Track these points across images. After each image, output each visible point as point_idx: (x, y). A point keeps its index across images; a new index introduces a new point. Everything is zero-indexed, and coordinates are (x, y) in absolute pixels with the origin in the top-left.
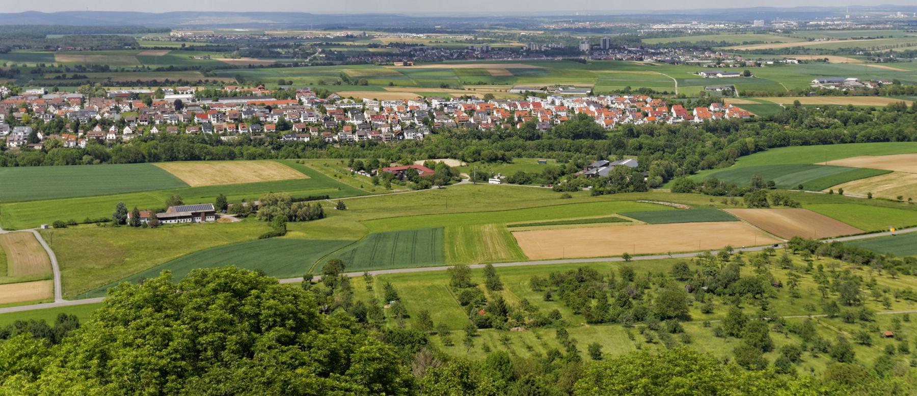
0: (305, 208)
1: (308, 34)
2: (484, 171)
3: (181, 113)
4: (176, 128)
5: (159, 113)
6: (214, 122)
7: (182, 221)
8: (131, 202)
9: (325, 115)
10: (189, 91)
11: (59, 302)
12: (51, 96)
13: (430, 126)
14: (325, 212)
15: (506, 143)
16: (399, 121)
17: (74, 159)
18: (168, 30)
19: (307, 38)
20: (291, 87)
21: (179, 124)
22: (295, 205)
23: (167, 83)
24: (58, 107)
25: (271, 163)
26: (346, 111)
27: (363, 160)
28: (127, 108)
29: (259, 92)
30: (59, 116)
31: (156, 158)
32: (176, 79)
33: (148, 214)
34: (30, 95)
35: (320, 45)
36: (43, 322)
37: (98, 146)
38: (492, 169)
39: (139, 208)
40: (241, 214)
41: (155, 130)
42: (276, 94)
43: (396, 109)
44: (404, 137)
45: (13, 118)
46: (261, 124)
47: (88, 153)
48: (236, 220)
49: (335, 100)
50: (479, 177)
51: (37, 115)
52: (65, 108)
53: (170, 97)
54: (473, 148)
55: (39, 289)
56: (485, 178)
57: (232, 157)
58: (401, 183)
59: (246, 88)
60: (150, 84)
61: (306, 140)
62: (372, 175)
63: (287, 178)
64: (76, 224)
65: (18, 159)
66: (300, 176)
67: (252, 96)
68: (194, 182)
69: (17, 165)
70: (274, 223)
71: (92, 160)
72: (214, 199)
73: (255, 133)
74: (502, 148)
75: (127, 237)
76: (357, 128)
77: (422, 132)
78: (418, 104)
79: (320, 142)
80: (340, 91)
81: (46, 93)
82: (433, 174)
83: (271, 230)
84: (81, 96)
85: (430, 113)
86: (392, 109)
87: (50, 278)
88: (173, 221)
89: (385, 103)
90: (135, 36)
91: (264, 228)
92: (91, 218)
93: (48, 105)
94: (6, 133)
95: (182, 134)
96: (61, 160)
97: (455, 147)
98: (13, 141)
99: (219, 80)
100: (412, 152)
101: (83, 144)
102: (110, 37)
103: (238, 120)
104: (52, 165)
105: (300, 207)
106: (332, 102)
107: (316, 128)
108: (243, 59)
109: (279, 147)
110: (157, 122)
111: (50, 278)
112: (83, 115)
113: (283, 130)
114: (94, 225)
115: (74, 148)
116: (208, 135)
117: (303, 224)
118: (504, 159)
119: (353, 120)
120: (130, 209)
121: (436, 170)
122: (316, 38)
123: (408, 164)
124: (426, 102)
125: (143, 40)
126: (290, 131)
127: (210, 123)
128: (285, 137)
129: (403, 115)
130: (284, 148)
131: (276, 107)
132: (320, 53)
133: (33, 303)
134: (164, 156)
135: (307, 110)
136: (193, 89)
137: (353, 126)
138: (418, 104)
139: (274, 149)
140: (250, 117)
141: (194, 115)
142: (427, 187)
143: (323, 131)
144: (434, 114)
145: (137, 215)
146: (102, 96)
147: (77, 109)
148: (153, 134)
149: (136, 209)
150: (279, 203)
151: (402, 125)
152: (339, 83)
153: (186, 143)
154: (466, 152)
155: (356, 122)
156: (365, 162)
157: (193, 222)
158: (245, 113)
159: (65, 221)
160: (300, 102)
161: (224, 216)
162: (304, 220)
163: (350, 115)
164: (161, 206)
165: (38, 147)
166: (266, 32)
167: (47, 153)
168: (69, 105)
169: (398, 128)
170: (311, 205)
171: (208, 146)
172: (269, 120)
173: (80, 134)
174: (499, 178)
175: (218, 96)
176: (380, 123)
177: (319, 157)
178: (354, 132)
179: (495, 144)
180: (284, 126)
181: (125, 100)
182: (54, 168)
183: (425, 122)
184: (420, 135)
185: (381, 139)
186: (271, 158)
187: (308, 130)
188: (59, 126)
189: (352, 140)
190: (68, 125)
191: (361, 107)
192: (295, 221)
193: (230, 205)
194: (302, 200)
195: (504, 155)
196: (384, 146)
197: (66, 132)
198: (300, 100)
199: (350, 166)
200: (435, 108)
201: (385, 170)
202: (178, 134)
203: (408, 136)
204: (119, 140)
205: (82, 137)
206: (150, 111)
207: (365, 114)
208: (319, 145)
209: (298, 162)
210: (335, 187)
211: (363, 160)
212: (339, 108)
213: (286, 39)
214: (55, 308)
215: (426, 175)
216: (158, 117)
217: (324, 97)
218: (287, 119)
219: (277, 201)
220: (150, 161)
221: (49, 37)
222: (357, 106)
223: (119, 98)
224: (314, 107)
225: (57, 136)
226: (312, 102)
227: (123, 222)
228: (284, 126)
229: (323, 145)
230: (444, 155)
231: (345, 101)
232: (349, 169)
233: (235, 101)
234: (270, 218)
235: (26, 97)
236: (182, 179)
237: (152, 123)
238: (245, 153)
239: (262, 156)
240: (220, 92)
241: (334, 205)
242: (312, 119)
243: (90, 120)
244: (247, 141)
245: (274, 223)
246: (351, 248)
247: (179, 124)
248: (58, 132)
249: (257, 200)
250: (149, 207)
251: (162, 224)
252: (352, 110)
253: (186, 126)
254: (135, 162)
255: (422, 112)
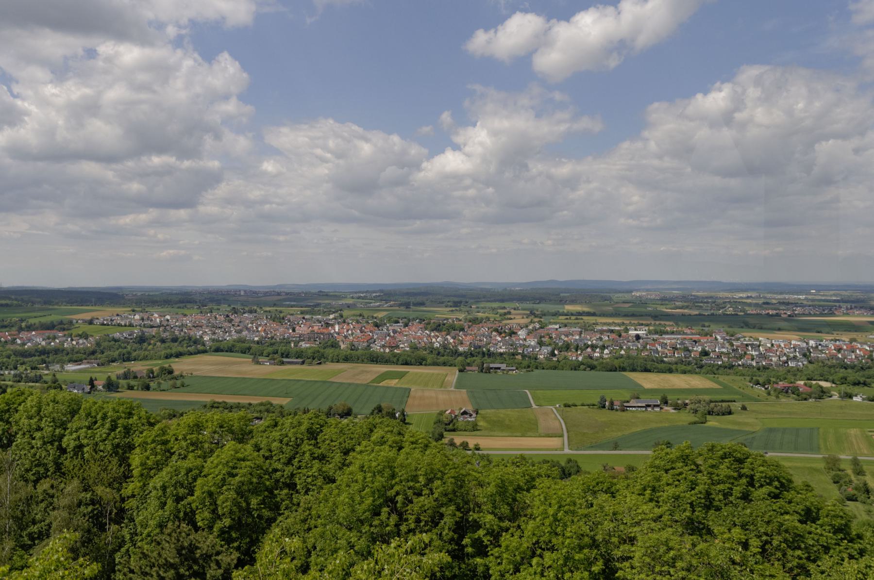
0: (719, 407)
1: (721, 294)
2: (849, 391)
3: (639, 342)
4: (636, 351)
5: (626, 342)
6: (659, 349)
7: (639, 409)
8: (609, 395)
9: (732, 348)
10: (644, 329)
11: (567, 451)
12: (563, 329)
13: (808, 358)
14: (733, 411)
15: (867, 372)
16: (785, 354)
17: (576, 367)
18: (631, 292)
19: (720, 298)
20: (710, 329)
21: (638, 349)
22: (712, 405)
23: (630, 324)
24: (567, 336)
25: (696, 376)
26: (747, 345)
27: (759, 378)
28: (607, 338)
29: (689, 331)
30: (567, 342)
31: (624, 369)
32: (636, 322)
33: (619, 403)
34: (551, 328)
35: (729, 302)
36: (558, 462)
37: (589, 360)
38: (856, 390)
39: (613, 399)
40: (677, 407)
41: (623, 352)
42: (700, 332)
43: (783, 346)
44: (788, 365)
45: (542, 341)
46: (688, 350)
47: (583, 364)
48: (673, 411)
49: (740, 338)
50: (846, 395)
51: (555, 340)
52: (570, 337)
53: (633, 332)
54: (841, 375)
55: (555, 442)
56: (851, 397)
57: (670, 371)
58: (786, 395)
59: (680, 329)
60: (619, 325)
61: (719, 363)
62: (766, 389)
63: (707, 387)
64: (576, 406)
65: (543, 365)
66: (716, 386)
67: (684, 334)
68: (647, 385)
69: (543, 369)
70: (699, 415)
71: (586, 368)
72: (660, 397)
73: (685, 357)
74: (863, 376)
75: (604, 416)
76: (755, 357)
77: (802, 362)
78: (799, 343)
79: (729, 365)
80: (743, 332)
81: (560, 327)
82: (809, 391)
83: (697, 419)
84: (580, 330)
85: (808, 350)
86: (780, 346)
87: (562, 436)
88: (634, 409)
89: (775, 341)
90: (611, 295)
91: (692, 418)
92: (585, 403)
93: (561, 334)
94: (538, 350)
95: (639, 355)
96: (568, 366)
97: (827, 373)
98: (541, 355)
99: (662, 323)
100: (795, 375)
101: (580, 359)
102: (596, 295)
103: (675, 348)
104: (563, 370)
105: (716, 406)
106: (738, 339)
107: (727, 356)
108: (678, 310)
109: (701, 367)
110: (625, 347)
111: (562, 436)
112: (581, 341)
113: (704, 356)
114: (587, 407)
115: (575, 360)
116: (655, 356)
117: (718, 417)
118: (865, 384)
119: (752, 351)
120: (608, 399)
121: (813, 387)
122: (727, 298)
123: (791, 383)
124: (805, 341)
125: (616, 297)
126: (709, 357)
127: (657, 349)
128: (705, 360)
129: (788, 350)
130: (704, 368)
131: (700, 341)
132: (729, 308)
133: (552, 450)
134: (628, 368)
135: (721, 344)
136: (647, 328)
137: (752, 355)
138: (799, 343)
139: (698, 367)
140: (682, 347)
141: (647, 344)
142: (805, 399)
143: (731, 358)
144: (811, 350)
145: (612, 403)
146: (592, 330)
147: (577, 337)
148: (622, 355)
149: (611, 399)
150: (702, 402)
151: (788, 356)
152: (742, 327)
153: (642, 361)
154: (835, 377)
155: (754, 353)
156: (761, 380)
157: (646, 410)
158: (679, 344)
159: (570, 403)
160: (716, 339)
161: (666, 408)
162: (718, 415)
163: (750, 348)
164: (627, 399)
165: (555, 359)
166: (693, 294)
167: (560, 362)
168: (573, 335)
169: (785, 358)
170: (723, 405)
171: (656, 363)
172: (695, 349)
173: (579, 352)
174: (861, 397)
175: (662, 333)
176: (771, 354)
177: (729, 375)
178: (753, 359)
179: (858, 373)
180: (705, 353)
181: (605, 333)
182: (564, 371)
183: (805, 355)
184: (800, 363)
185: (772, 365)
186: (696, 373)
187: (721, 356)
188: (567, 347)
189: (751, 365)
190: (572, 347)
191: (758, 343)
192: (712, 415)
193: (669, 402)
194: (717, 402)
195: (865, 381)
196: (774, 370)
197: (571, 351)
198: (716, 337)
199: (750, 382)
200: (812, 347)
201: (775, 386)
202: (637, 355)
203: (791, 364)
204: (601, 357)
205: (580, 355)
206: (620, 340)
207: (761, 348)
208: (728, 366)
209: (714, 377)
210: (740, 395)
211: (759, 378)
212: (742, 344)
213: (707, 298)
214: (564, 454)
215: (805, 391)
216: (625, 344)
217: (732, 336)
218: (707, 349)
219: (701, 401)
220: (620, 371)
221: (562, 295)
222: (755, 343)
223: (602, 332)
224: (725, 342)
225: (566, 353)
226: (724, 339)
227: (604, 407)
228: (705, 353)
229: (731, 367)
230: (818, 379)
231: (747, 339)
232: (749, 384)
233: (673, 336)
234: (696, 411)
235: (549, 329)
236: (640, 383)
237: (621, 348)
238: (679, 370)
239: (690, 372)
240: (664, 330)
241: (739, 407)
242: (724, 350)
243: (585, 344)
244: (680, 361)
245: (699, 415)
246: (750, 436)
247: (638, 349)
248: (567, 351)
249: (687, 399)
250: (621, 399)
251: (627, 410)
252: (752, 345)
253: (642, 351)
254: (611, 371)
255: (802, 348)
